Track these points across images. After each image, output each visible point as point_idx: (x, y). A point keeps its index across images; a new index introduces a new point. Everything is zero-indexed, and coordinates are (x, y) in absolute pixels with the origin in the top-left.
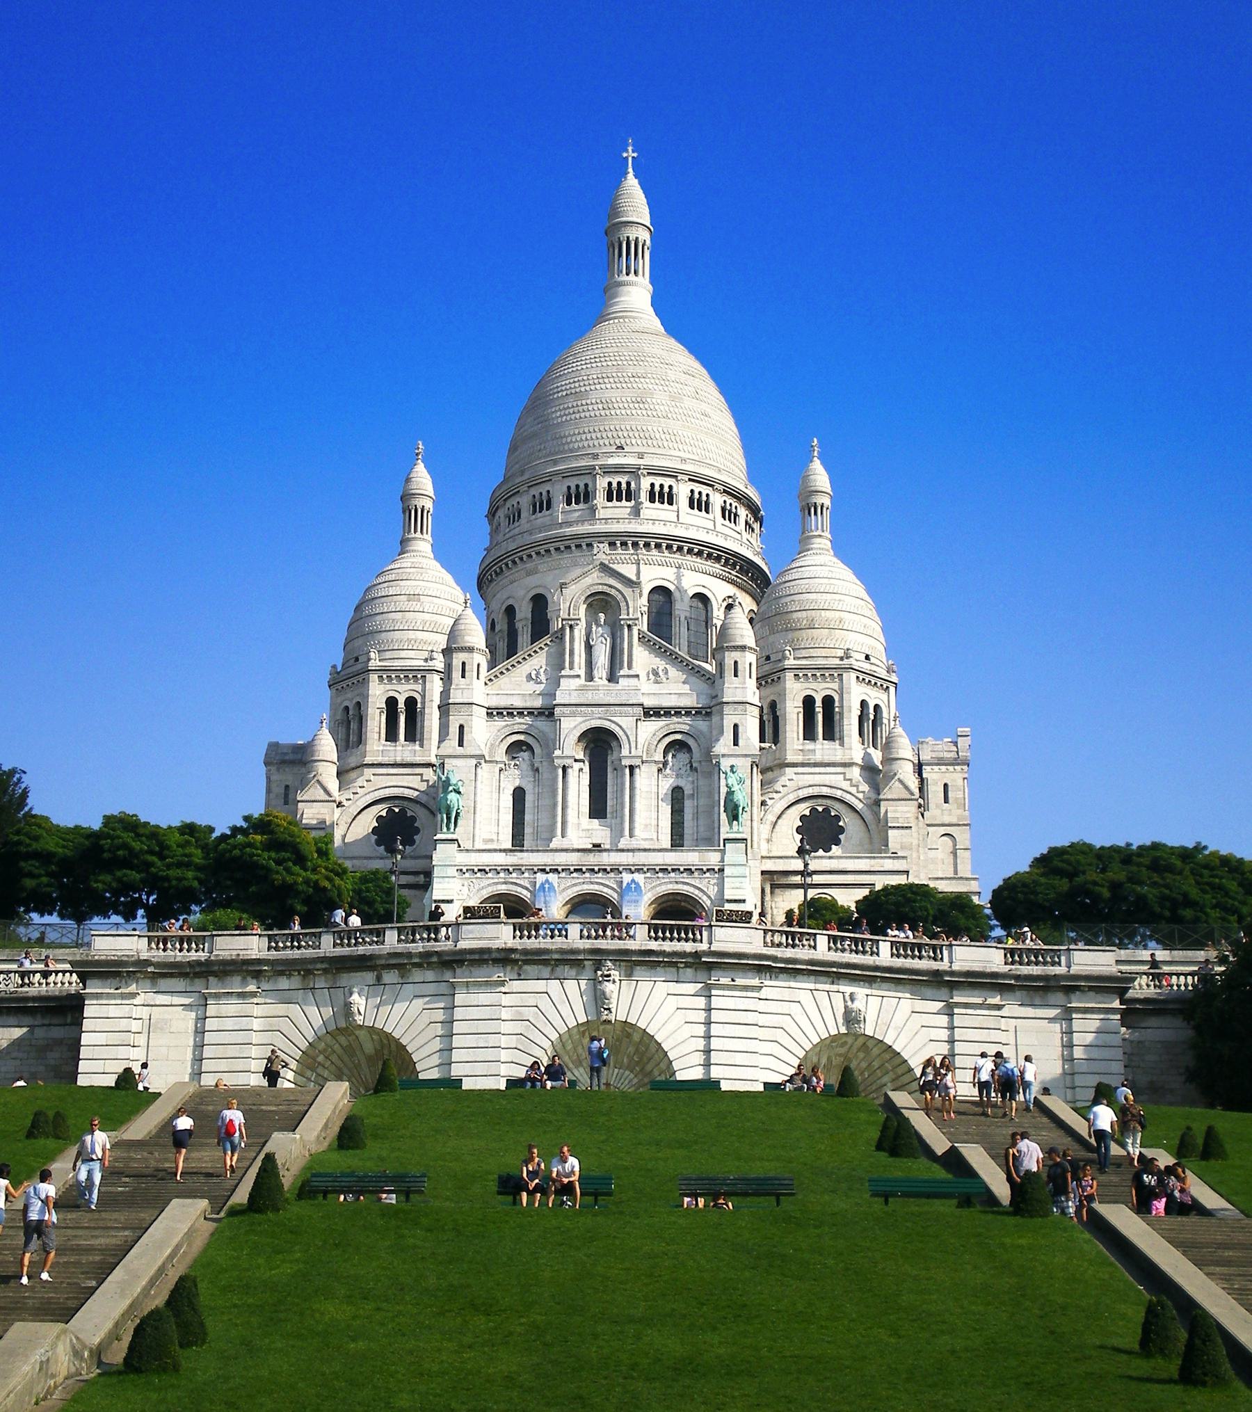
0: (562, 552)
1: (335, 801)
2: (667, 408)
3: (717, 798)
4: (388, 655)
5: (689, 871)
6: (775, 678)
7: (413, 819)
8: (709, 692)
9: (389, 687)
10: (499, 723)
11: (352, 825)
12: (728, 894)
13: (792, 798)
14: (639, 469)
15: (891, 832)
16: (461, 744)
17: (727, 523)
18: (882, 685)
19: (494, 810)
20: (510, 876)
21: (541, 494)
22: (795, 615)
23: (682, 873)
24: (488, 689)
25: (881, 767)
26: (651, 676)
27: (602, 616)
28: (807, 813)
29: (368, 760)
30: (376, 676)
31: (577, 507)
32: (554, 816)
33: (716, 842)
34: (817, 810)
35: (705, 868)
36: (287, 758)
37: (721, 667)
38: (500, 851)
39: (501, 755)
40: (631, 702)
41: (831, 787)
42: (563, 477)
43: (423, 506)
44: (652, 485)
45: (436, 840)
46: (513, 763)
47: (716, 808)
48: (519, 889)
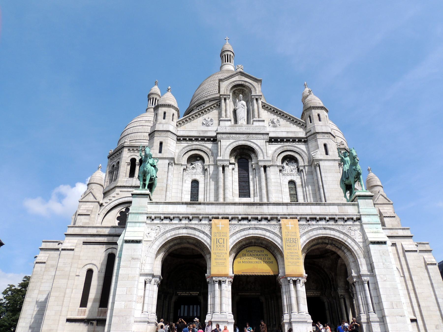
1: (98, 202)
3: (321, 184)
4: (134, 141)
9: (132, 154)
12: (371, 237)
16: (160, 152)
19: (179, 191)
20: (190, 222)
23: (328, 221)
24: (179, 129)
26: (270, 124)
27: (241, 95)
29: (119, 184)
30: (127, 149)
35: (346, 218)
38: (183, 203)
39: (184, 160)
40: (262, 132)
43: (156, 98)
47: (322, 190)
48: (197, 233)
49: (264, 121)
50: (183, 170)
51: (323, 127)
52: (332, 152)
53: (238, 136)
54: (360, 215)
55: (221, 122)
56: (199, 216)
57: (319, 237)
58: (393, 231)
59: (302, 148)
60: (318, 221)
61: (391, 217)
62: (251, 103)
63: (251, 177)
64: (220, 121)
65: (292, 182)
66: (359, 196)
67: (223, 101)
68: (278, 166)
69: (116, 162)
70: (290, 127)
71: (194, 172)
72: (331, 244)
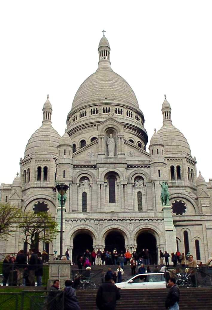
0: (90, 127)
1: (21, 199)
7: (47, 205)
8: (149, 160)
9: (38, 163)
10: (78, 170)
11: (27, 208)
15: (203, 208)
16: (64, 177)
17: (137, 121)
18: (193, 163)
21: (83, 112)
25: (196, 188)
27: (111, 135)
28: (174, 202)
29: (32, 186)
30: (35, 160)
31: (94, 115)
32: (97, 202)
33: (155, 210)
34: (177, 201)
36: (6, 188)
39: (78, 181)
41: (182, 194)
42: (90, 107)
44: (116, 109)
45: (57, 209)
47: (154, 199)
48: (89, 227)
49: (124, 154)
53: (109, 165)
54: (164, 217)
55: (99, 155)
58: (203, 217)
59: (146, 172)
60: (144, 220)
61: (207, 206)
62: (117, 141)
63: (116, 190)
64: (98, 154)
65: (139, 193)
68: (132, 184)
69: (27, 168)
70: (141, 157)
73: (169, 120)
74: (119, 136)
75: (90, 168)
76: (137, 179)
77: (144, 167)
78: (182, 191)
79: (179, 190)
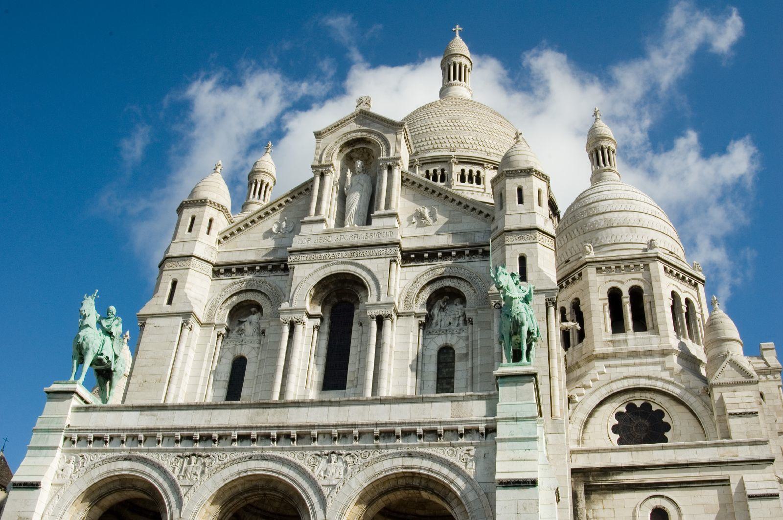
2: (476, 126)
5: (432, 433)
6: (577, 276)
12: (504, 470)
13: (604, 392)
14: (451, 158)
15: (733, 422)
18: (690, 281)
22: (593, 219)
24: (222, 248)
26: (414, 220)
28: (623, 409)
35: (461, 428)
37: (500, 197)
39: (222, 317)
40: (384, 241)
41: (649, 378)
44: (463, 171)
46: (237, 330)
49: (395, 215)
50: (218, 336)
51: (522, 215)
52: (536, 274)
53: (331, 254)
56: (156, 433)
57: (395, 474)
58: (727, 448)
62: (378, 178)
66: (503, 376)
67: (318, 179)
70: (460, 222)
71: (241, 339)
72: (426, 489)
73: (609, 170)
74: (383, 160)
75: (271, 271)
76: (440, 303)
77: (468, 256)
78: (651, 368)
79: (641, 365)
